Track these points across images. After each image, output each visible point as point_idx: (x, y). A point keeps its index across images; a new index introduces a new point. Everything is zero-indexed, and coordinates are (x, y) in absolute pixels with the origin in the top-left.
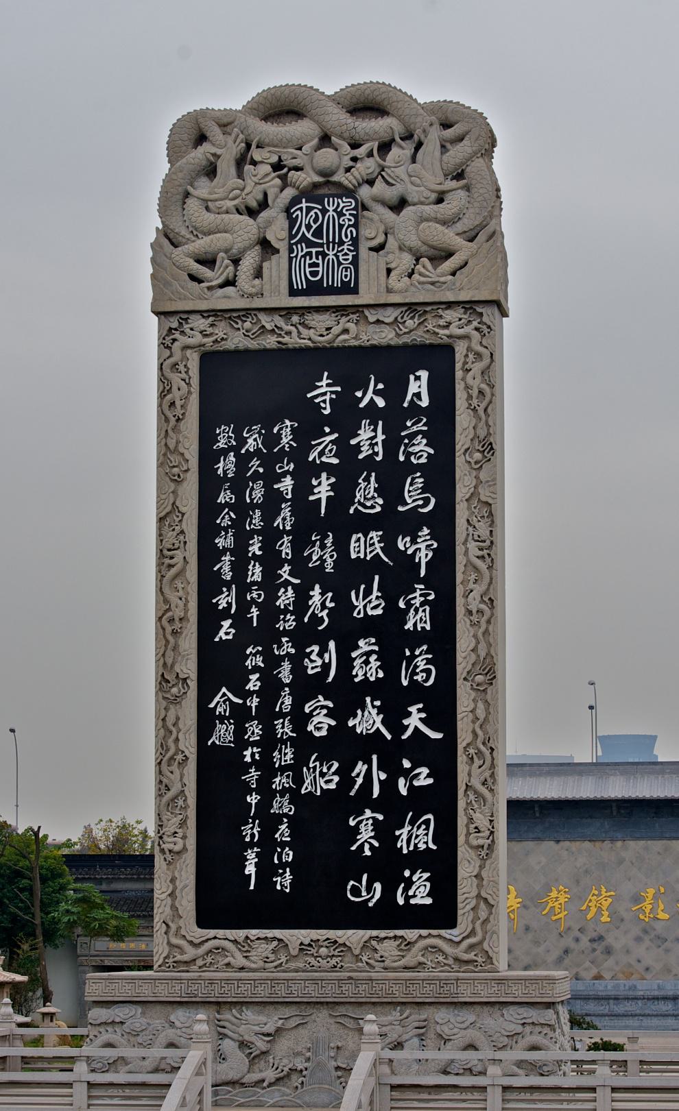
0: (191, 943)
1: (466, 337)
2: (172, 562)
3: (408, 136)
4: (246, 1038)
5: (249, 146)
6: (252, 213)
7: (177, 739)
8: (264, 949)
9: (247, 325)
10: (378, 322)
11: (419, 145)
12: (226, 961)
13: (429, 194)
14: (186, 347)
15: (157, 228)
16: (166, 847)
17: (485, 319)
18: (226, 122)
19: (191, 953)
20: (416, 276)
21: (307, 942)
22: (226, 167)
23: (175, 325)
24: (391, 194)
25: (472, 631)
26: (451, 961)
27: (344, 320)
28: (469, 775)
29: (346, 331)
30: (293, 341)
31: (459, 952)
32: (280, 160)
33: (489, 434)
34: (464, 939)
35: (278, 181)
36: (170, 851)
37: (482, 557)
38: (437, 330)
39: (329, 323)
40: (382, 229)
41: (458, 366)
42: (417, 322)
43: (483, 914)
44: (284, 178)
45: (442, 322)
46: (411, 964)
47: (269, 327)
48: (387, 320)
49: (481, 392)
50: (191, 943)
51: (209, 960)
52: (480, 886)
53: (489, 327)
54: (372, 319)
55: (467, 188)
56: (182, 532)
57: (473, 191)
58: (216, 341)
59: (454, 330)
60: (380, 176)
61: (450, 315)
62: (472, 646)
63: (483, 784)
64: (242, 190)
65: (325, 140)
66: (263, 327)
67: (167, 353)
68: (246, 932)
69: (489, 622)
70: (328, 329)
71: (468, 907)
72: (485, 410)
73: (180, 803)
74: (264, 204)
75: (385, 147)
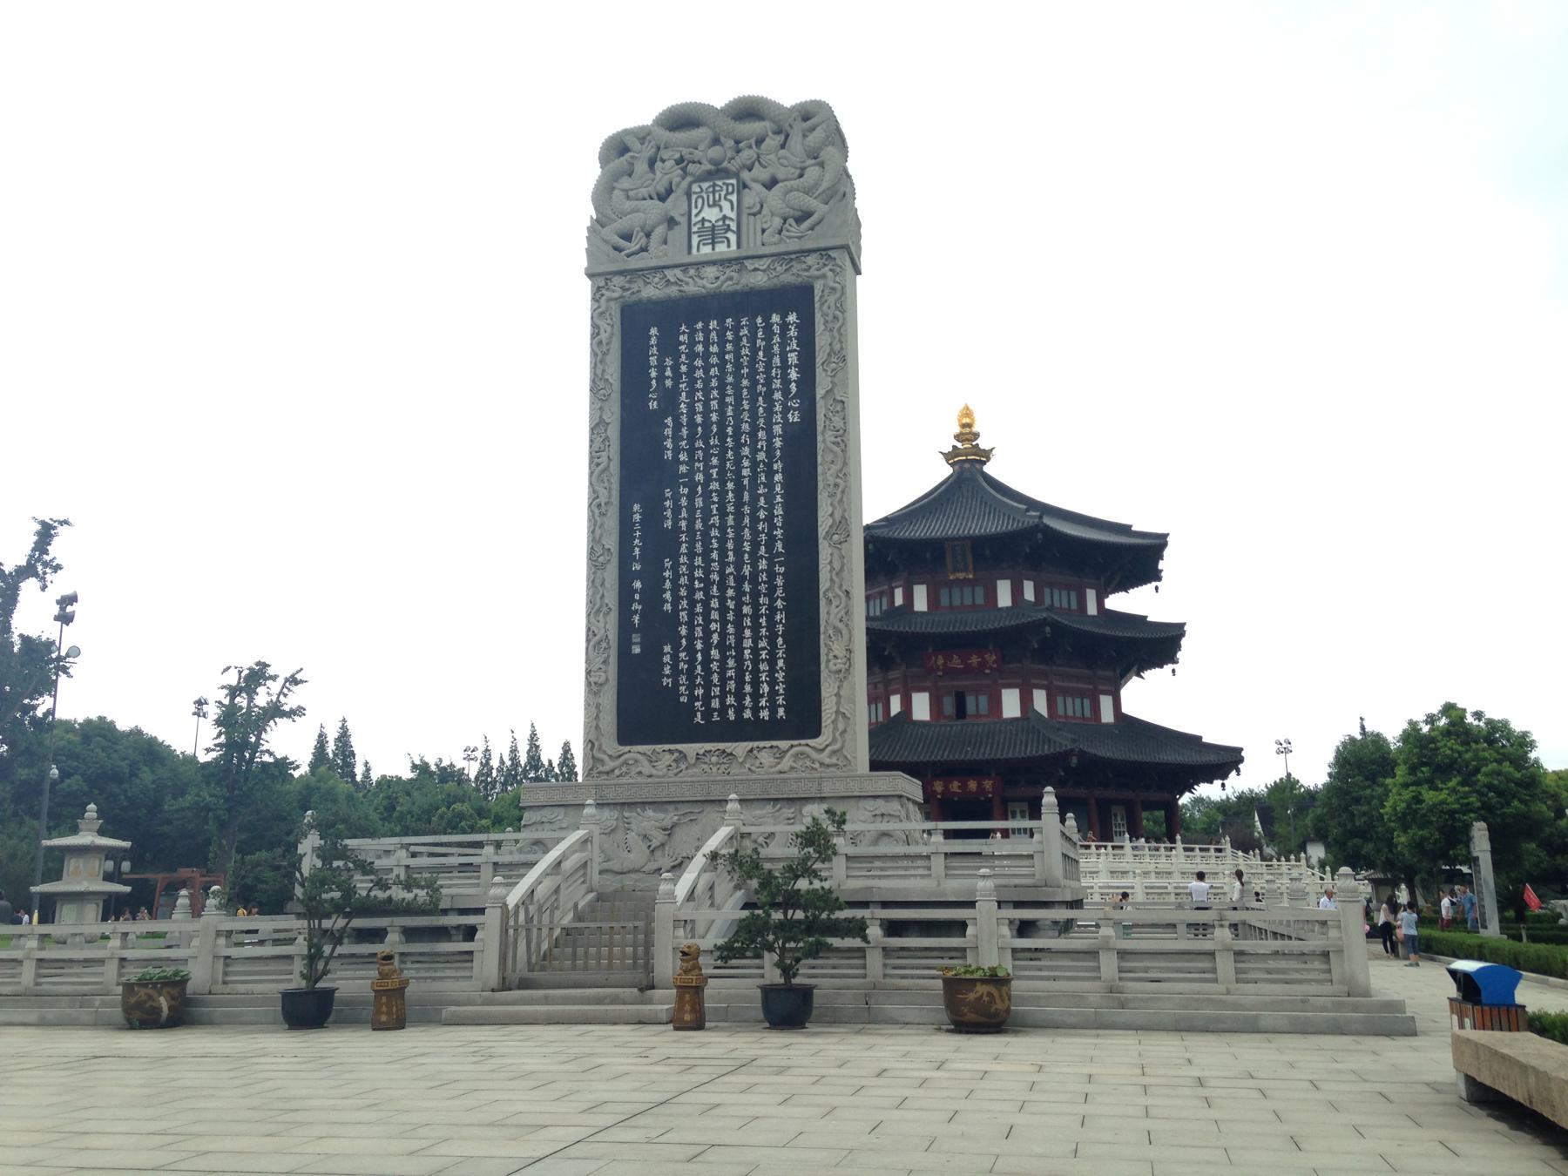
0: (610, 756)
1: (824, 276)
2: (600, 461)
3: (778, 132)
4: (649, 832)
5: (659, 149)
6: (662, 198)
7: (603, 596)
8: (668, 759)
9: (656, 280)
10: (756, 270)
11: (787, 136)
12: (638, 770)
13: (793, 170)
14: (610, 299)
15: (592, 217)
16: (592, 680)
17: (838, 261)
18: (642, 135)
19: (610, 764)
20: (784, 233)
21: (701, 752)
22: (641, 167)
23: (602, 284)
24: (764, 175)
25: (829, 501)
26: (817, 765)
27: (728, 271)
28: (828, 613)
29: (731, 278)
30: (691, 288)
31: (824, 757)
32: (682, 156)
33: (842, 348)
34: (827, 746)
35: (679, 171)
36: (595, 683)
37: (837, 444)
38: (800, 273)
39: (717, 274)
40: (757, 200)
41: (817, 299)
42: (785, 268)
43: (841, 727)
44: (684, 170)
45: (804, 266)
46: (786, 769)
47: (672, 280)
48: (761, 268)
49: (835, 317)
50: (610, 756)
51: (624, 769)
52: (838, 703)
53: (840, 267)
54: (750, 267)
55: (822, 165)
56: (607, 438)
57: (826, 167)
58: (633, 293)
59: (813, 272)
60: (757, 163)
61: (811, 260)
62: (830, 512)
63: (841, 621)
64: (653, 180)
65: (716, 141)
66: (668, 280)
67: (596, 305)
68: (654, 747)
69: (843, 492)
70: (717, 278)
71: (829, 721)
72: (839, 329)
73: (604, 645)
74: (669, 191)
75: (759, 142)
